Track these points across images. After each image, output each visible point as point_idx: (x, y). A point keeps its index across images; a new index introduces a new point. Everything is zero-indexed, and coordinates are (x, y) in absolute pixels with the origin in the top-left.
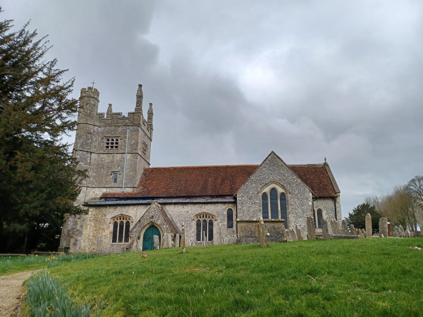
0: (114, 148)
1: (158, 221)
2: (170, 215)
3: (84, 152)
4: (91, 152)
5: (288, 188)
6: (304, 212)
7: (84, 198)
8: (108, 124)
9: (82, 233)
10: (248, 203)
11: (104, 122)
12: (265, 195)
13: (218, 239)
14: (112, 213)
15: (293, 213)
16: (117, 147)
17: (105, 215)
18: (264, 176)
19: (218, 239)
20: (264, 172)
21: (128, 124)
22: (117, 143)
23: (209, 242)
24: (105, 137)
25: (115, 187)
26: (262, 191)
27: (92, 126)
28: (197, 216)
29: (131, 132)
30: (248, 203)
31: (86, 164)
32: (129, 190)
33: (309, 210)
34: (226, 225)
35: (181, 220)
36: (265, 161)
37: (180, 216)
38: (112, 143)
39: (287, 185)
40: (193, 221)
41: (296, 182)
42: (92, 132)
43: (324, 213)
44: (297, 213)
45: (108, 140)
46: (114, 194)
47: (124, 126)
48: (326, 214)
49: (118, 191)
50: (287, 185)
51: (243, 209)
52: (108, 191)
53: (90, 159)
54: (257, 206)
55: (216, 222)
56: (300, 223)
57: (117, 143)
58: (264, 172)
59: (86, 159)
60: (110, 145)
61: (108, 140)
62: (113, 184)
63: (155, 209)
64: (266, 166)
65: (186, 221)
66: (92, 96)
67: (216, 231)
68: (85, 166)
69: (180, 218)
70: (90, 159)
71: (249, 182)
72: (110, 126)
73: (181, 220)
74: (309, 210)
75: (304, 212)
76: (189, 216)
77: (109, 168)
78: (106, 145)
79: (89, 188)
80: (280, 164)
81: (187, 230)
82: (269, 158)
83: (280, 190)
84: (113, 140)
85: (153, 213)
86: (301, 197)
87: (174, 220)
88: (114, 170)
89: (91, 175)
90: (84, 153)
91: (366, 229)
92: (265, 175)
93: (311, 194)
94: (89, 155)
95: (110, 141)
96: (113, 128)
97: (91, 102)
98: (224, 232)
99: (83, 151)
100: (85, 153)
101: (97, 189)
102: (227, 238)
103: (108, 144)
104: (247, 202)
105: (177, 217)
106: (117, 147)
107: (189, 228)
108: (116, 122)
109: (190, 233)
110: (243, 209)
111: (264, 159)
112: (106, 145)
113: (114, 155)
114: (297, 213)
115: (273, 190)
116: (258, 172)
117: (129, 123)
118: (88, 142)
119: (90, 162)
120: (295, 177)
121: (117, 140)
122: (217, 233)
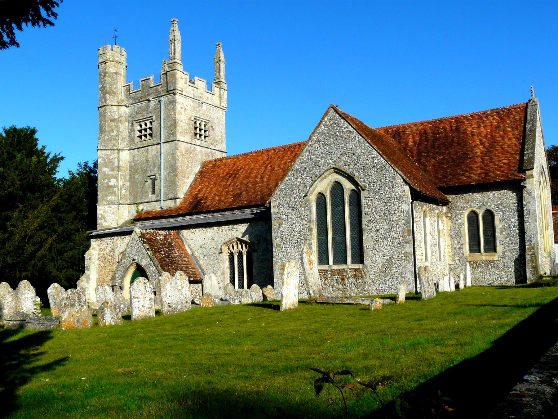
0: (148, 137)
1: (142, 261)
3: (108, 151)
4: (118, 150)
5: (361, 178)
6: (391, 227)
7: (116, 222)
8: (137, 99)
9: (89, 278)
10: (290, 216)
11: (133, 98)
12: (321, 198)
14: (120, 246)
15: (370, 231)
16: (151, 135)
17: (113, 250)
18: (317, 159)
20: (317, 152)
21: (162, 92)
22: (151, 129)
24: (135, 121)
25: (152, 202)
26: (314, 190)
27: (115, 108)
28: (227, 244)
29: (166, 106)
30: (290, 216)
31: (112, 170)
32: (170, 204)
33: (404, 221)
35: (205, 254)
36: (317, 127)
38: (145, 130)
39: (359, 174)
41: (377, 164)
42: (116, 117)
43: (497, 218)
44: (378, 230)
45: (141, 126)
46: (148, 213)
47: (157, 97)
48: (502, 220)
49: (156, 207)
50: (359, 174)
51: (282, 229)
52: (145, 208)
53: (119, 161)
54: (305, 223)
56: (383, 250)
57: (151, 129)
58: (317, 152)
59: (111, 162)
60: (143, 132)
61: (141, 126)
62: (153, 197)
63: (138, 242)
64: (320, 138)
65: (212, 255)
66: (111, 59)
68: (111, 173)
69: (203, 251)
70: (119, 161)
71: (290, 176)
72: (139, 102)
73: (205, 254)
74: (404, 221)
75: (391, 227)
77: (144, 171)
78: (138, 134)
79: (121, 206)
80: (346, 129)
82: (326, 119)
83: (348, 186)
84: (146, 124)
85: (136, 247)
86: (387, 196)
87: (196, 254)
88: (150, 174)
89: (123, 186)
90: (109, 152)
91: (275, 286)
92: (317, 158)
93: (407, 188)
94: (116, 155)
95: (144, 126)
96: (144, 103)
97: (111, 70)
99: (106, 150)
100: (109, 153)
101: (132, 205)
103: (140, 131)
104: (287, 216)
106: (151, 135)
108: (147, 94)
110: (282, 229)
111: (317, 124)
112: (138, 134)
113: (148, 149)
114: (378, 230)
115: (337, 188)
116: (305, 155)
117: (162, 91)
118: (112, 134)
119: (118, 164)
120: (375, 154)
121: (151, 123)
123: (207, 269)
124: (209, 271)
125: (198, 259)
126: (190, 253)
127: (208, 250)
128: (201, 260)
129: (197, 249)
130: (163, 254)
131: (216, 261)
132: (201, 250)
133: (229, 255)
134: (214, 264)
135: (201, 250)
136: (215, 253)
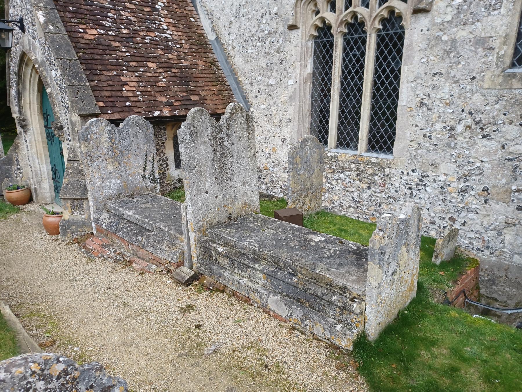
2: (210, 14)
13: (420, 146)
19: (420, 146)
23: (369, 154)
34: (496, 44)
37: (243, 11)
40: (294, 34)
55: (424, 20)
67: (414, 89)
69: (243, 27)
76: (275, 10)
81: (268, 85)
87: (226, 38)
98: (477, 99)
102: (492, 145)
105: (234, 22)
107: (275, 74)
109: (279, 102)
122: (422, 104)
123: (251, 83)
124: (255, 89)
125: (232, 53)
126: (211, 37)
127: (255, 23)
128: (238, 56)
129: (227, 24)
130: (109, 29)
131: (275, 59)
132: (238, 25)
133: (316, 34)
134: (269, 67)
135: (236, 25)
136: (276, 32)
